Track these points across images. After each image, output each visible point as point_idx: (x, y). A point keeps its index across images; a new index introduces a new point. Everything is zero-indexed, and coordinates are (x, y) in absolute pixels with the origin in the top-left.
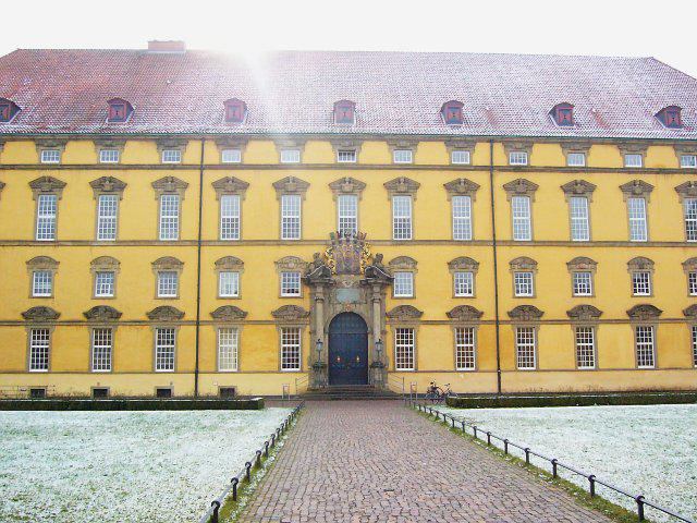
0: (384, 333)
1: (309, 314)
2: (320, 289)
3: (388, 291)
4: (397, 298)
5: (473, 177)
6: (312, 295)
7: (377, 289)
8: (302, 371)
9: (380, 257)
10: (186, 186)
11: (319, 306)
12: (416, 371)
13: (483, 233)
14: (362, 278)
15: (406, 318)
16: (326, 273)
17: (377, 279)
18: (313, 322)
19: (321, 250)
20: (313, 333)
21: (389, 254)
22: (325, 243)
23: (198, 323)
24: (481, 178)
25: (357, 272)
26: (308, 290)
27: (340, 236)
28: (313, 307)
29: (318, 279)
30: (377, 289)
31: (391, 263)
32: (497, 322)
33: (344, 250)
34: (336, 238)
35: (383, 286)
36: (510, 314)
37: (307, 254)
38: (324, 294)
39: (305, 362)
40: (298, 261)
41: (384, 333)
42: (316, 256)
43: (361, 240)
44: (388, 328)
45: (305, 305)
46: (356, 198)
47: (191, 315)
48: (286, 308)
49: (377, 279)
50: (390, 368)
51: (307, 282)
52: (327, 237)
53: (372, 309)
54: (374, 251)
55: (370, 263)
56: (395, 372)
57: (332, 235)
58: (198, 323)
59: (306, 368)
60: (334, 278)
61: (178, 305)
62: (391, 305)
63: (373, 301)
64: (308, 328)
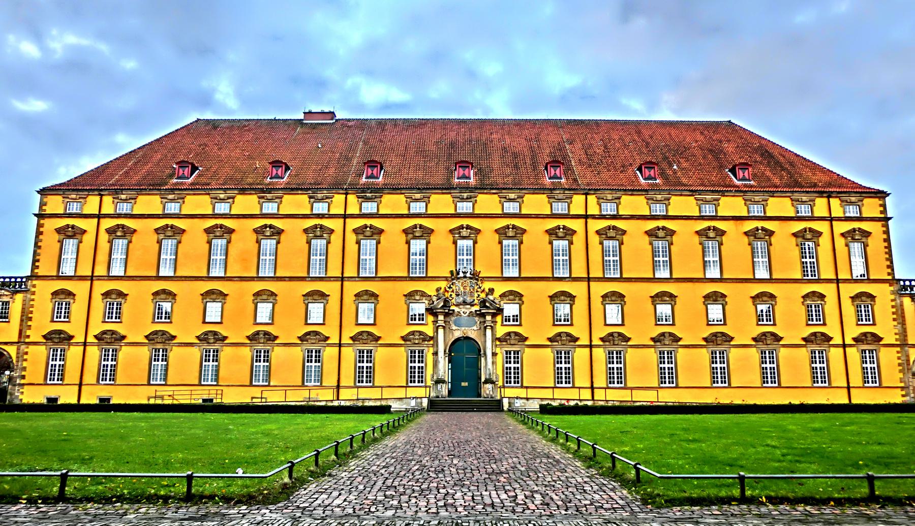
0: (494, 354)
1: (431, 338)
2: (441, 317)
3: (499, 319)
7: (489, 318)
8: (426, 387)
11: (441, 331)
13: (335, 272)
14: (477, 308)
15: (512, 342)
18: (436, 345)
23: (340, 345)
24: (577, 225)
25: (471, 304)
26: (431, 318)
27: (458, 274)
30: (489, 318)
32: (591, 346)
35: (494, 315)
36: (602, 339)
38: (445, 322)
40: (423, 294)
42: (438, 290)
44: (498, 350)
45: (429, 330)
46: (425, 241)
50: (500, 383)
55: (483, 295)
56: (504, 387)
58: (340, 345)
60: (452, 308)
62: (501, 331)
63: (485, 328)
64: (431, 350)
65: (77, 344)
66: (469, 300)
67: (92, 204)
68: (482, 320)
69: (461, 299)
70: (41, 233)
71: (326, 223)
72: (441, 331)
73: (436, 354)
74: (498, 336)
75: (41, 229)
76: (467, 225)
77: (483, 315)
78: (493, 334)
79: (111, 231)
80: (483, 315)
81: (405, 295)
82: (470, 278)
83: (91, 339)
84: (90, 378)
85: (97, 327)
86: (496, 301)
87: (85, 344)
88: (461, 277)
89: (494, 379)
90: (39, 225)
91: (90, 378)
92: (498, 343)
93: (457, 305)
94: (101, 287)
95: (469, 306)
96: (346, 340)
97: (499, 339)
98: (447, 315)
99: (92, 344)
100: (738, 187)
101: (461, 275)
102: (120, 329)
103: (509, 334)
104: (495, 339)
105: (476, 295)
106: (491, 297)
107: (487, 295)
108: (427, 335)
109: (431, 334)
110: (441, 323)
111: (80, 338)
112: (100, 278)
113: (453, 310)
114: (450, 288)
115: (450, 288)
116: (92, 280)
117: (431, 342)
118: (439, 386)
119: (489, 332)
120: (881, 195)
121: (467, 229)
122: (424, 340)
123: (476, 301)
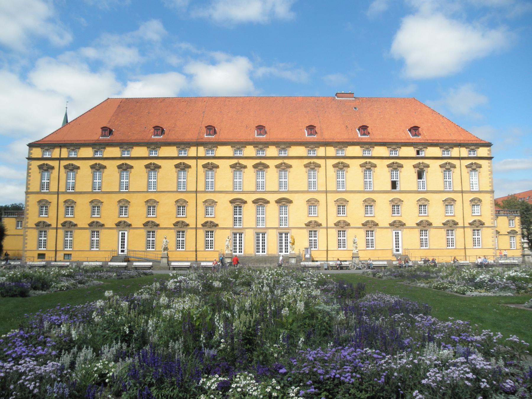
5: (318, 161)
10: (189, 167)
23: (196, 228)
47: (192, 225)
58: (196, 228)
61: (187, 221)
65: (53, 229)
67: (56, 153)
70: (30, 169)
71: (187, 162)
75: (30, 167)
79: (66, 167)
83: (60, 226)
84: (60, 246)
85: (61, 220)
87: (57, 228)
90: (29, 165)
91: (60, 246)
94: (62, 198)
96: (199, 226)
99: (60, 228)
100: (413, 139)
102: (74, 221)
111: (54, 225)
112: (63, 193)
116: (58, 194)
120: (488, 145)
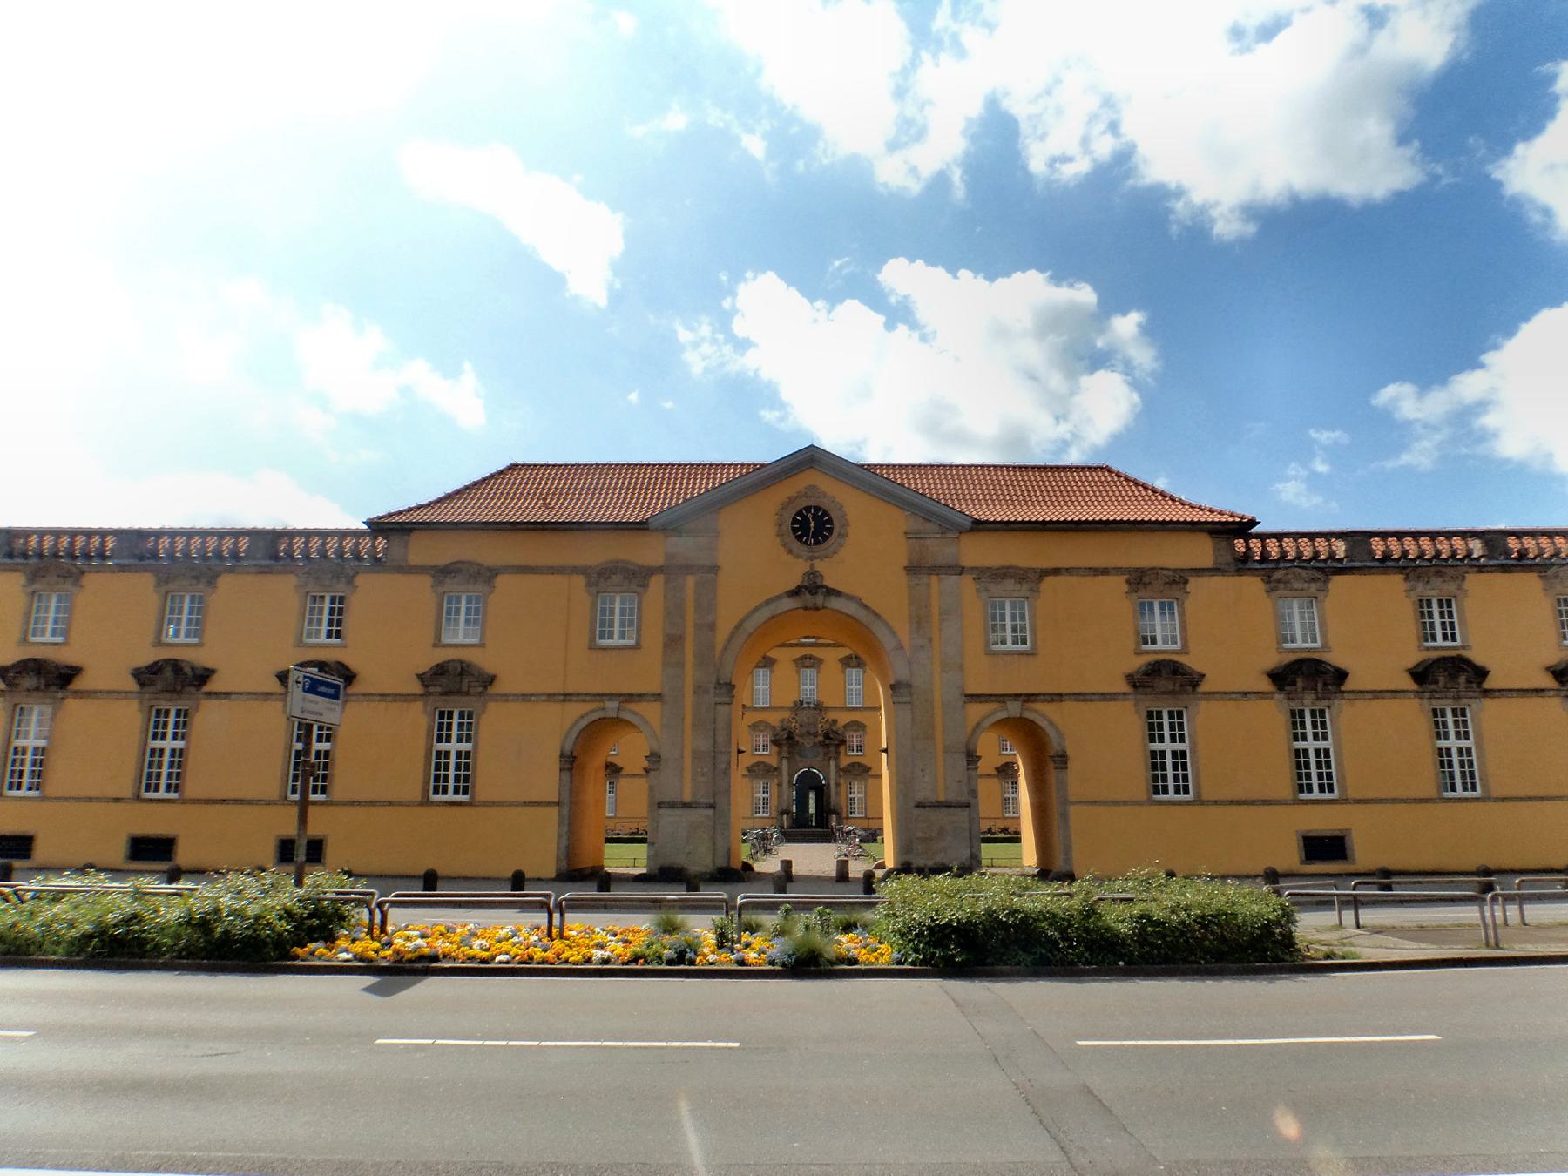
1: (776, 769)
2: (785, 749)
3: (842, 749)
4: (850, 756)
6: (779, 753)
7: (832, 749)
9: (835, 722)
12: (866, 818)
14: (821, 738)
15: (856, 773)
16: (790, 737)
17: (833, 741)
19: (787, 715)
20: (780, 785)
21: (843, 719)
22: (790, 709)
26: (775, 749)
27: (802, 703)
28: (780, 762)
29: (786, 740)
30: (832, 749)
31: (846, 726)
33: (804, 716)
34: (799, 705)
35: (838, 746)
37: (774, 719)
38: (789, 754)
39: (773, 808)
40: (767, 725)
41: (838, 785)
42: (782, 721)
43: (819, 707)
44: (842, 781)
48: (758, 764)
49: (833, 741)
50: (844, 815)
51: (776, 742)
52: (792, 705)
53: (829, 765)
54: (831, 716)
55: (826, 726)
57: (795, 703)
59: (774, 815)
60: (797, 739)
62: (844, 762)
64: (776, 781)
66: (813, 731)
68: (826, 750)
69: (804, 730)
72: (785, 763)
73: (780, 785)
74: (842, 767)
76: (811, 655)
77: (827, 746)
78: (837, 766)
80: (827, 746)
81: (749, 726)
82: (814, 708)
86: (840, 732)
88: (804, 708)
89: (839, 811)
92: (842, 773)
93: (801, 736)
95: (812, 737)
97: (842, 770)
98: (791, 746)
101: (805, 705)
103: (853, 765)
104: (839, 769)
105: (820, 726)
106: (834, 728)
107: (831, 725)
108: (772, 767)
109: (775, 764)
110: (786, 754)
113: (798, 742)
114: (794, 718)
115: (794, 718)
117: (776, 773)
118: (785, 816)
119: (832, 763)
121: (810, 658)
122: (768, 771)
123: (820, 732)
